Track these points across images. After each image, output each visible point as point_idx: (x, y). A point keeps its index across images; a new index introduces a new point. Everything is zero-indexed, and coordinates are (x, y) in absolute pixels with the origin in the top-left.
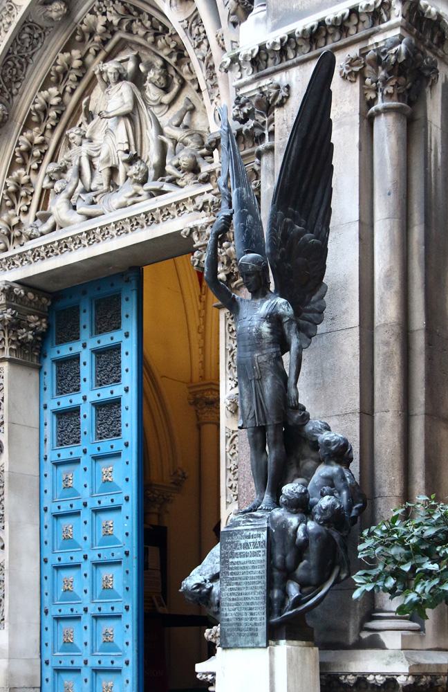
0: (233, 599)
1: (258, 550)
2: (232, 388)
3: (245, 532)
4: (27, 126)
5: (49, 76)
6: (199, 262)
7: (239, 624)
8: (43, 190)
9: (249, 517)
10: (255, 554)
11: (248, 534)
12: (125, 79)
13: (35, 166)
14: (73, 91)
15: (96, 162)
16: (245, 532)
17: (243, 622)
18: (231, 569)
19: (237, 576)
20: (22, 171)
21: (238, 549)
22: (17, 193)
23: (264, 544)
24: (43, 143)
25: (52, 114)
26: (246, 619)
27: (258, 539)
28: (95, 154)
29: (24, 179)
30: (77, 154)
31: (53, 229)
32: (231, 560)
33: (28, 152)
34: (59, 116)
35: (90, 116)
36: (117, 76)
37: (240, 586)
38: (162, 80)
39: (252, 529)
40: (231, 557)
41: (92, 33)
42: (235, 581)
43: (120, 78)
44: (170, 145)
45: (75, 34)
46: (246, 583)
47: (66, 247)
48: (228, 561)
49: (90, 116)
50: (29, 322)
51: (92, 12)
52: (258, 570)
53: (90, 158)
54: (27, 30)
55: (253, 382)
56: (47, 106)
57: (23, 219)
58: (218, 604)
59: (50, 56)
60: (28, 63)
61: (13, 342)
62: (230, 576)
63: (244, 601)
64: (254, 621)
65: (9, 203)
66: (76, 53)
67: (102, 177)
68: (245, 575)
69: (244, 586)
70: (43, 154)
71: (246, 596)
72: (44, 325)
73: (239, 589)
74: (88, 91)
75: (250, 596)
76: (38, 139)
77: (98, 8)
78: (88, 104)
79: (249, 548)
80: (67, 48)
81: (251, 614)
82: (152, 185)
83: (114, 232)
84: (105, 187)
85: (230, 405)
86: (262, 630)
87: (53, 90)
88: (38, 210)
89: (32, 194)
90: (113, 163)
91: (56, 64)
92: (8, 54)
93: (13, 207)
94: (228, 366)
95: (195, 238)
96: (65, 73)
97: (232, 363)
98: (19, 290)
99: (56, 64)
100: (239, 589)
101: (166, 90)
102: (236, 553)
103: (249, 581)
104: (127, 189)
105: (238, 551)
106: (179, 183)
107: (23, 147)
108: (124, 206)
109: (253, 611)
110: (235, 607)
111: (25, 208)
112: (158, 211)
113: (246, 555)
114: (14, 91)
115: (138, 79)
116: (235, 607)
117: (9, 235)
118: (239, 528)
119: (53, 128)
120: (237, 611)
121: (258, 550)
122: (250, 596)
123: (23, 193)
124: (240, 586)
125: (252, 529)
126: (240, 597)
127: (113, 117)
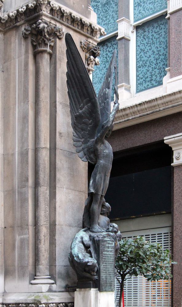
0: (105, 270)
3: (108, 241)
7: (106, 281)
10: (111, 251)
16: (108, 241)
39: (110, 241)
40: (103, 251)
48: (102, 253)
79: (109, 249)
81: (110, 277)
103: (110, 262)
109: (111, 276)
113: (108, 251)
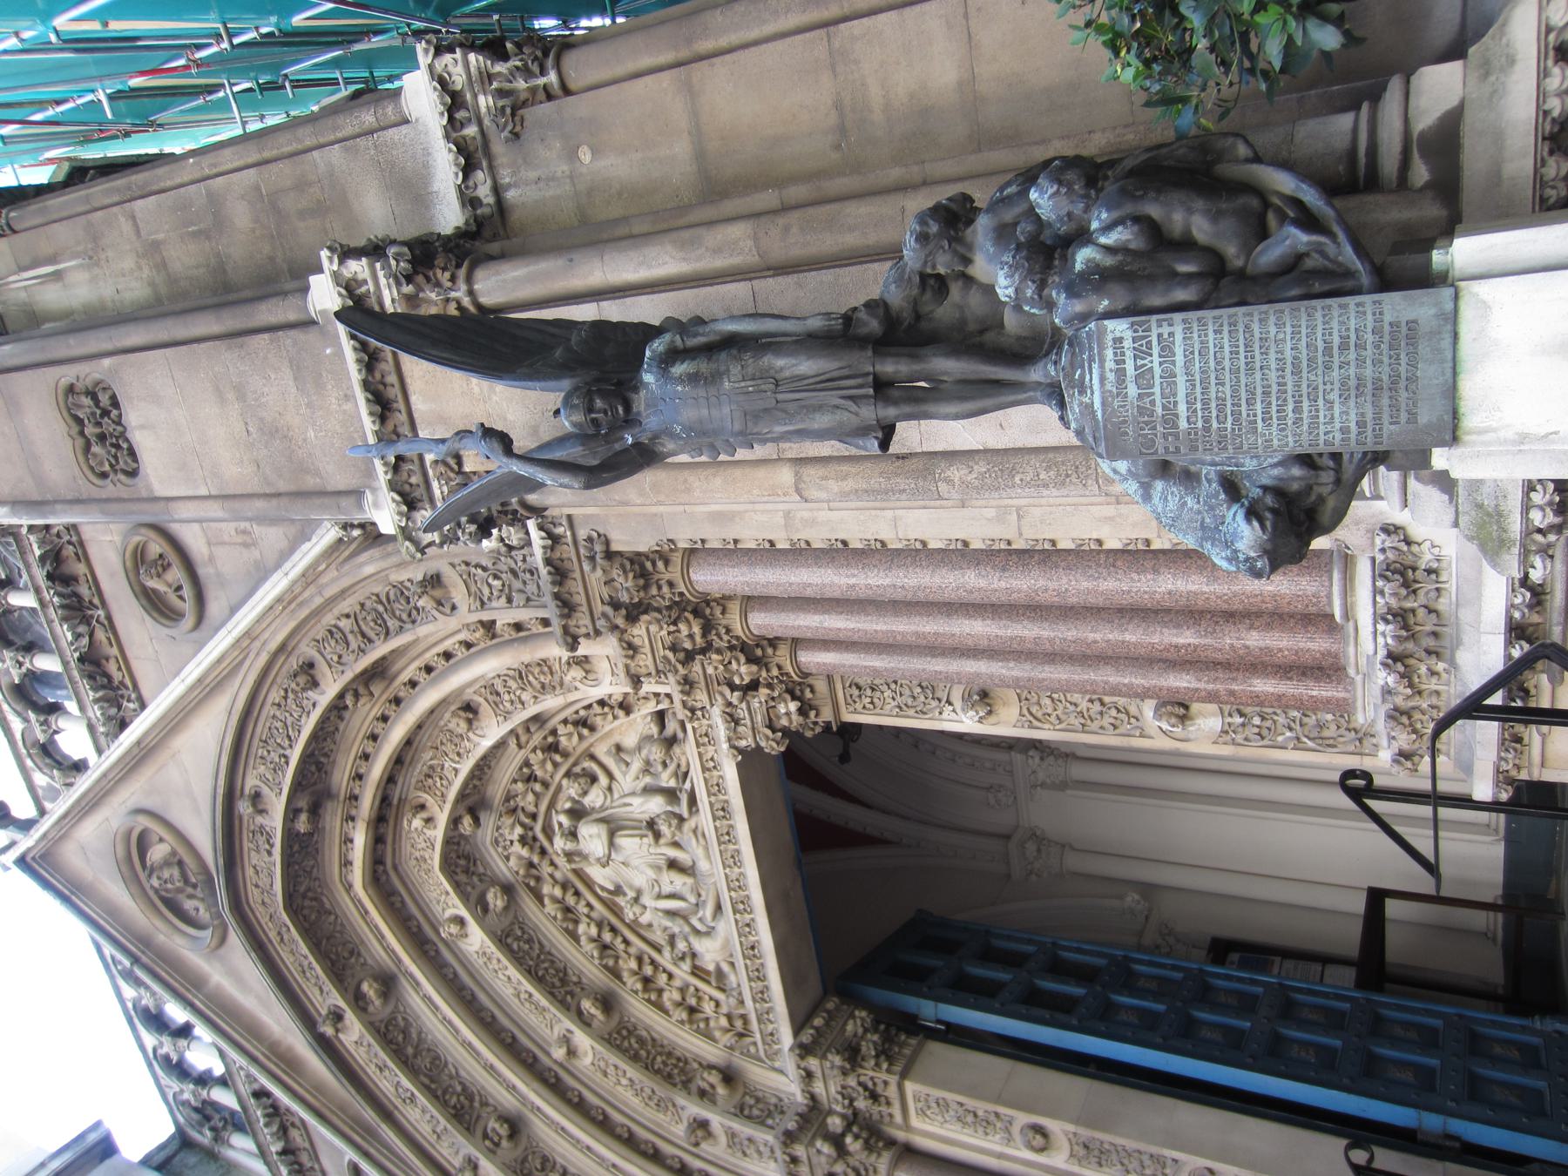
1: (1155, 343)
3: (1109, 387)
4: (615, 973)
5: (566, 930)
8: (693, 974)
10: (1167, 350)
11: (1111, 376)
13: (664, 977)
14: (589, 905)
15: (667, 889)
16: (1109, 387)
17: (1368, 372)
18: (1207, 420)
20: (666, 995)
21: (1153, 403)
22: (692, 1010)
23: (1140, 324)
24: (640, 960)
25: (607, 937)
26: (1361, 362)
27: (1128, 343)
28: (657, 889)
29: (677, 996)
30: (651, 913)
31: (732, 964)
32: (1183, 424)
33: (647, 981)
34: (613, 930)
35: (618, 891)
37: (1259, 391)
38: (582, 780)
39: (1102, 366)
41: (531, 865)
42: (1244, 408)
43: (573, 835)
44: (648, 780)
45: (528, 885)
47: (753, 948)
49: (618, 891)
50: (855, 1035)
51: (507, 858)
52: (1211, 336)
53: (659, 896)
54: (509, 940)
55: (780, 397)
56: (596, 940)
57: (724, 1010)
58: (1307, 460)
59: (543, 919)
60: (549, 953)
61: (877, 1065)
62: (1229, 425)
63: (1304, 375)
64: (1369, 338)
65: (702, 1025)
66: (546, 889)
67: (679, 882)
69: (1258, 375)
70: (653, 962)
72: (864, 1014)
73: (1266, 394)
74: (589, 883)
75: (1288, 354)
76: (633, 965)
77: (505, 848)
78: (603, 888)
80: (539, 898)
81: (1344, 347)
82: (683, 809)
83: (736, 870)
84: (690, 881)
86: (1396, 306)
87: (582, 928)
88: (708, 982)
89: (697, 990)
90: (663, 863)
91: (555, 918)
92: (529, 972)
93: (707, 1020)
95: (743, 743)
96: (567, 910)
98: (806, 1037)
99: (555, 918)
100: (1266, 394)
101: (594, 779)
102: (1164, 407)
104: (692, 852)
105: (1158, 403)
106: (683, 769)
107: (639, 986)
108: (706, 848)
109: (1336, 340)
110: (1321, 402)
111: (713, 1004)
112: (713, 799)
113: (1169, 376)
114: (575, 979)
116: (1321, 402)
117: (741, 1035)
118: (1097, 405)
119: (626, 942)
120: (1334, 396)
121: (1155, 343)
122: (1288, 354)
123: (693, 1002)
124: (1259, 391)
125: (1102, 366)
126: (1290, 387)
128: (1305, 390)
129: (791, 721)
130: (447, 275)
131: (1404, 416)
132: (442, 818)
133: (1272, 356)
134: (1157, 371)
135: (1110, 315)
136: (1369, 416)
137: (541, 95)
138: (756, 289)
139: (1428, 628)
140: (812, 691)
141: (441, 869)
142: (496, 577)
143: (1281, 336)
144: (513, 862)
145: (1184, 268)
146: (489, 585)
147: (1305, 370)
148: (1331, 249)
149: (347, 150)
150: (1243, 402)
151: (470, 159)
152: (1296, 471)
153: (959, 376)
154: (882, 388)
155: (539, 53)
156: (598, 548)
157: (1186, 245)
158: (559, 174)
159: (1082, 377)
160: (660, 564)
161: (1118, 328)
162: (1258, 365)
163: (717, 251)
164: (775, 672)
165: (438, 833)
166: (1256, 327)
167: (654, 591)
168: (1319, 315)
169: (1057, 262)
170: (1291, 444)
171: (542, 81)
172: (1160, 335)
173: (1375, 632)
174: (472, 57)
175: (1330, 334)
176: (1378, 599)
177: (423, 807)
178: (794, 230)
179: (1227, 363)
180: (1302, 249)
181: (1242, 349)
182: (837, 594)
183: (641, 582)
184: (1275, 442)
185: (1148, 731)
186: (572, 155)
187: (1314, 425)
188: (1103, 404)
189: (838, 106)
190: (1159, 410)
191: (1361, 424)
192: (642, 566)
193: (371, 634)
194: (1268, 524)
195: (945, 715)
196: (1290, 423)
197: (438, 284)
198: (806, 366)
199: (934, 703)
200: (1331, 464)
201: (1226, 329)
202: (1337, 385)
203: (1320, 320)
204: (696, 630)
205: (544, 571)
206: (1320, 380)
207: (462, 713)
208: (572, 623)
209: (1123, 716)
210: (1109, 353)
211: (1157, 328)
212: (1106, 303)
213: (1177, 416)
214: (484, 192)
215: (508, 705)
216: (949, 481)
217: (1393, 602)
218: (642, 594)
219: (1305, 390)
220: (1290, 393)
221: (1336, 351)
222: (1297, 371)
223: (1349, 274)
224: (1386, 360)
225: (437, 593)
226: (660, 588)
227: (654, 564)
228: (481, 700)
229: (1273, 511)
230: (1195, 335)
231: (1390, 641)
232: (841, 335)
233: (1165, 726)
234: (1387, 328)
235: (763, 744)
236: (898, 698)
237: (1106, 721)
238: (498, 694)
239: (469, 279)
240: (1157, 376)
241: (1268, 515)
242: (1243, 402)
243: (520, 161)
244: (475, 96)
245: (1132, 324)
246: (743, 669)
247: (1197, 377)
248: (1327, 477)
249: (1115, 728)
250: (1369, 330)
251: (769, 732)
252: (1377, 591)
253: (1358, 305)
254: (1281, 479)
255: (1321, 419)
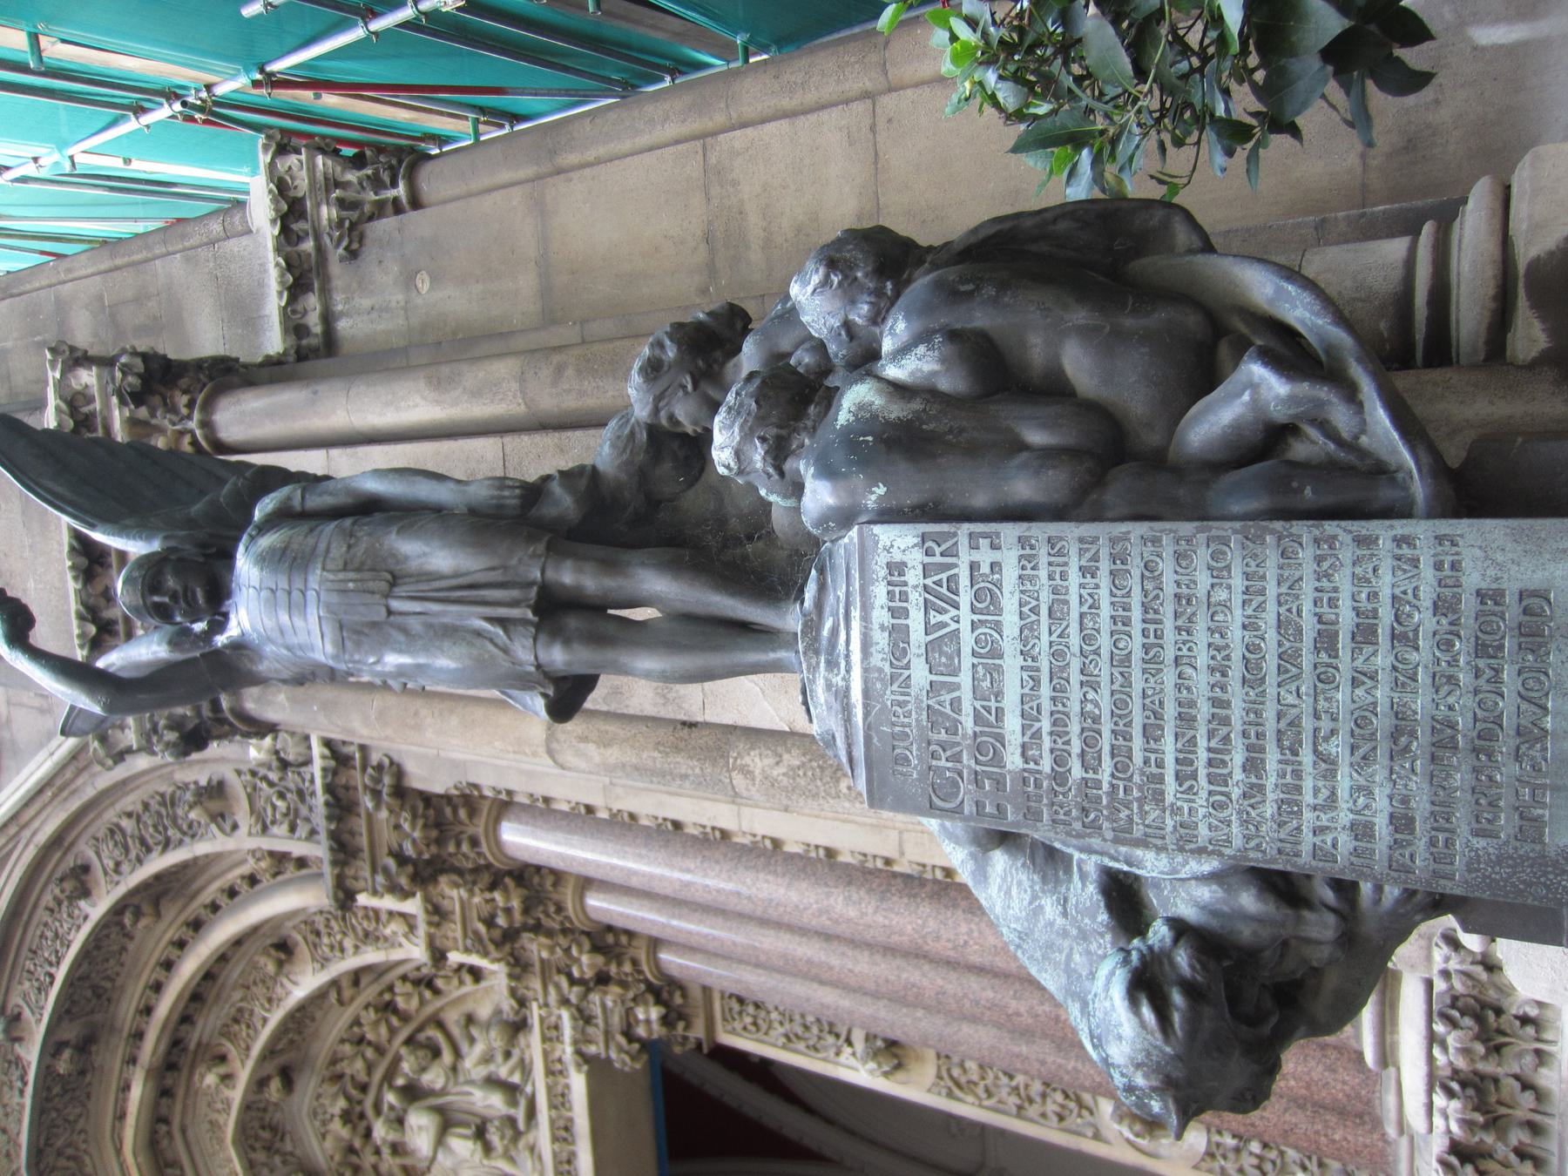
0: (1253, 765)
1: (964, 581)
2: (854, 1054)
3: (876, 660)
6: (627, 1053)
9: (816, 639)
10: (987, 600)
11: (881, 639)
12: (405, 1111)
17: (1421, 703)
18: (1060, 760)
19: (1106, 728)
21: (956, 704)
26: (1403, 677)
27: (913, 577)
36: (396, 1125)
37: (1170, 711)
38: (421, 1053)
40: (998, 760)
41: (351, 1150)
42: (1138, 743)
43: (400, 1121)
46: (1152, 663)
51: (324, 1136)
62: (1105, 776)
63: (1271, 691)
64: (1425, 621)
68: (1104, 670)
69: (1169, 677)
71: (1236, 671)
73: (1186, 720)
75: (1236, 635)
77: (324, 1123)
81: (1365, 634)
82: (520, 1114)
85: (880, 1065)
94: (812, 1053)
95: (592, 1049)
97: (811, 1043)
100: (1186, 720)
101: (436, 1053)
102: (978, 719)
105: (967, 706)
110: (1306, 756)
115: (412, 1093)
116: (1306, 756)
118: (856, 695)
120: (1337, 747)
121: (964, 581)
122: (1236, 635)
124: (1170, 711)
126: (1237, 714)
127: (435, 1152)
128: (1270, 727)
129: (650, 1030)
130: (184, 399)
131: (1506, 823)
132: (244, 1075)
133: (1201, 637)
134: (967, 640)
135: (889, 515)
136: (1421, 806)
137: (390, 208)
138: (508, 449)
139: (1521, 1114)
140: (684, 996)
141: (234, 1142)
142: (282, 796)
143: (1221, 595)
144: (329, 1143)
145: (1036, 437)
146: (274, 807)
147: (1272, 679)
148: (1341, 416)
149: (187, 260)
150: (1137, 731)
151: (302, 277)
152: (1248, 900)
153: (681, 607)
154: (553, 610)
155: (394, 162)
156: (387, 780)
157: (1052, 390)
158: (393, 304)
159: (835, 632)
160: (462, 813)
161: (899, 540)
162: (1169, 654)
163: (476, 394)
164: (627, 968)
165: (236, 1095)
166: (1167, 567)
167: (451, 848)
168: (1306, 555)
169: (812, 410)
170: (1238, 842)
171: (390, 194)
172: (974, 567)
173: (1430, 1106)
174: (320, 159)
175: (1332, 603)
176: (1436, 1052)
177: (223, 1059)
178: (570, 372)
179: (1105, 642)
180: (1280, 414)
181: (1136, 614)
182: (668, 891)
183: (434, 833)
184: (1203, 831)
185: (1105, 1133)
186: (409, 281)
187: (1290, 804)
188: (866, 693)
189: (708, 239)
190: (968, 723)
191: (1402, 822)
192: (440, 812)
193: (150, 841)
194: (1176, 1018)
195: (842, 1059)
196: (1236, 793)
197: (173, 409)
198: (438, 557)
199: (830, 1039)
200: (1329, 895)
201: (1105, 566)
202: (1345, 726)
203: (1308, 569)
204: (516, 904)
205: (320, 798)
206: (1306, 705)
207: (273, 952)
208: (350, 872)
209: (1072, 1105)
210: (880, 592)
211: (970, 548)
212: (881, 490)
213: (1000, 738)
214: (314, 321)
215: (326, 949)
216: (746, 772)
217: (1461, 1063)
218: (434, 849)
219: (1270, 727)
220: (1237, 724)
221: (1344, 640)
222: (1254, 677)
223: (1380, 471)
224: (1464, 678)
225: (215, 806)
226: (458, 845)
227: (455, 811)
228: (299, 938)
229: (1189, 988)
230: (1043, 573)
231: (1454, 1127)
232: (513, 516)
233: (1128, 1134)
234: (1468, 604)
235: (613, 1055)
236: (787, 1026)
237: (1051, 1107)
238: (318, 934)
239: (208, 406)
240: (966, 650)
241: (1177, 998)
242: (1137, 731)
243: (355, 285)
244: (318, 205)
245: (924, 538)
246: (585, 959)
247: (1044, 664)
248: (1321, 927)
249: (1061, 1118)
250: (1426, 600)
251: (622, 1040)
252: (1432, 1038)
253: (1399, 541)
254: (1215, 913)
255: (1308, 798)
